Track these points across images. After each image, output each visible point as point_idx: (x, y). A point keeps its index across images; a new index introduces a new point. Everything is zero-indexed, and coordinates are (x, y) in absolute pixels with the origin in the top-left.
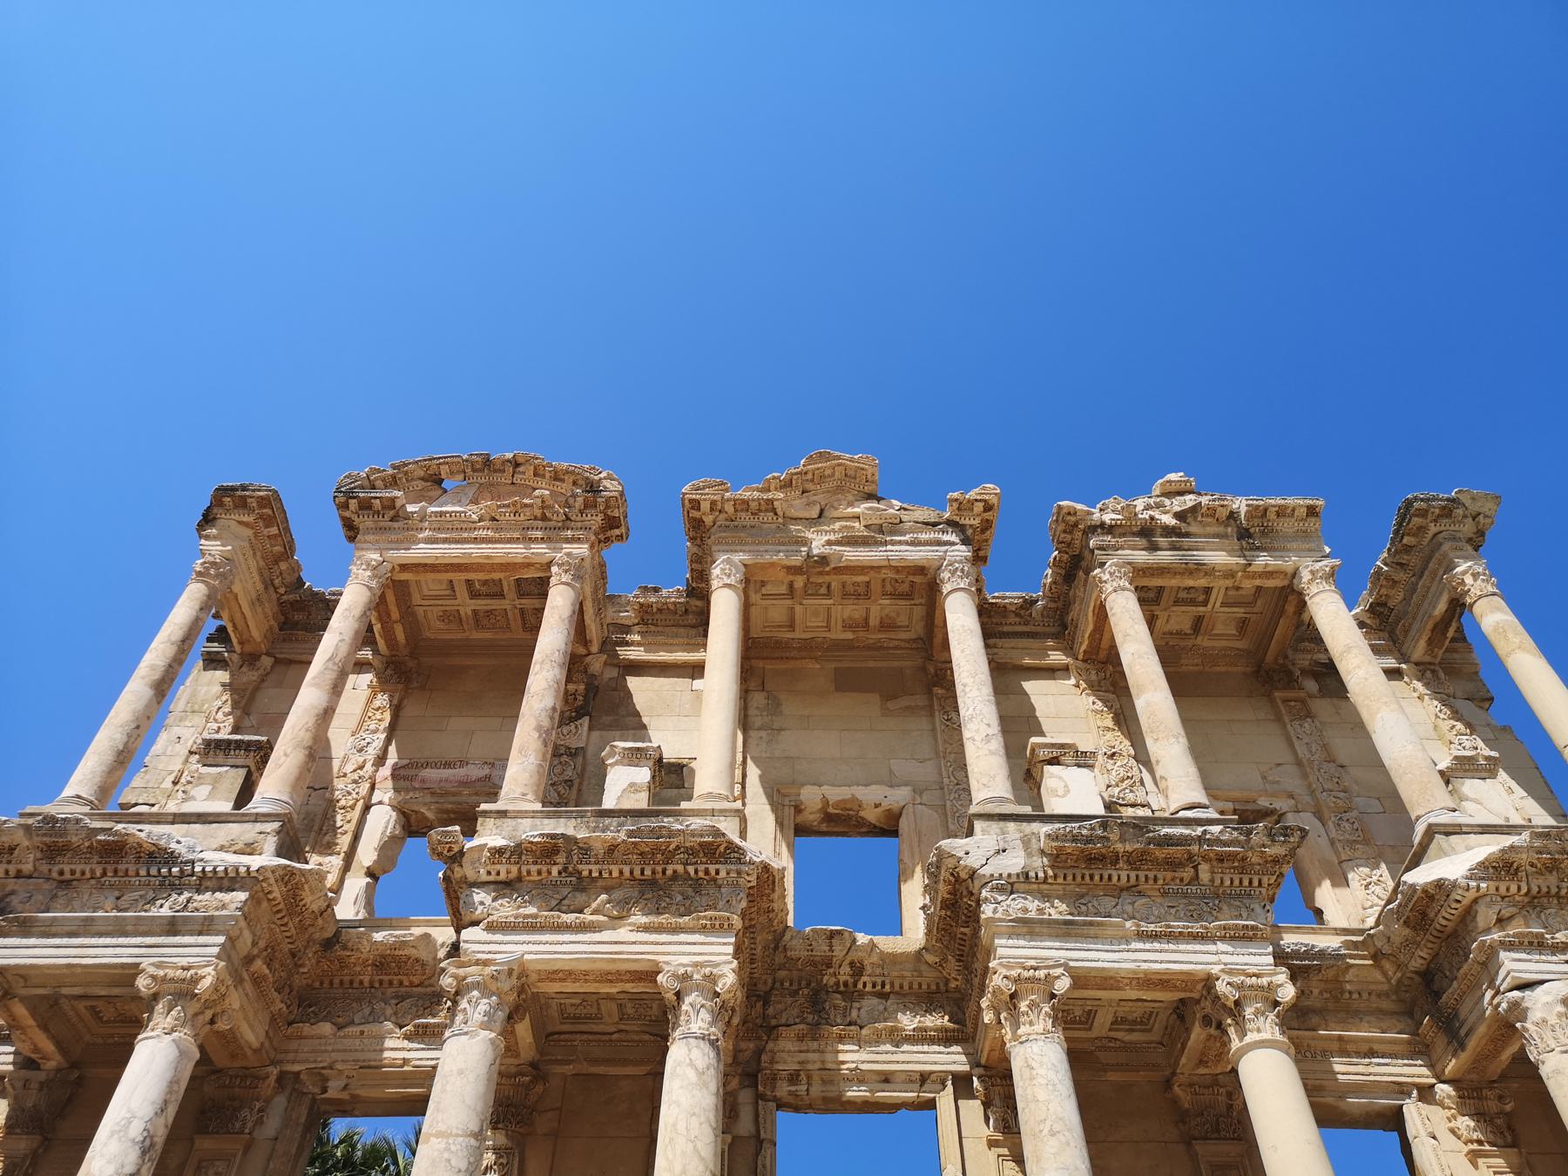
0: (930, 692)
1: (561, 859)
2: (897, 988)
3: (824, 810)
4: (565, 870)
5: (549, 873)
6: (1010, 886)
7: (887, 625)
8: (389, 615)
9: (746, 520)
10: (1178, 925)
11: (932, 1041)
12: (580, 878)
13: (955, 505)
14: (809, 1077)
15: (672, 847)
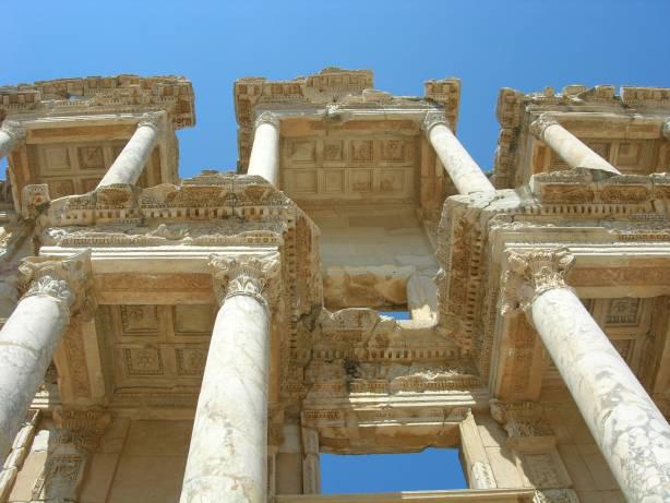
0: (421, 225)
1: (128, 205)
2: (418, 355)
3: (346, 284)
4: (132, 212)
5: (118, 216)
6: (511, 216)
7: (386, 187)
8: (23, 178)
9: (281, 98)
10: (650, 232)
11: (450, 387)
12: (143, 220)
13: (430, 87)
14: (346, 415)
15: (223, 194)
